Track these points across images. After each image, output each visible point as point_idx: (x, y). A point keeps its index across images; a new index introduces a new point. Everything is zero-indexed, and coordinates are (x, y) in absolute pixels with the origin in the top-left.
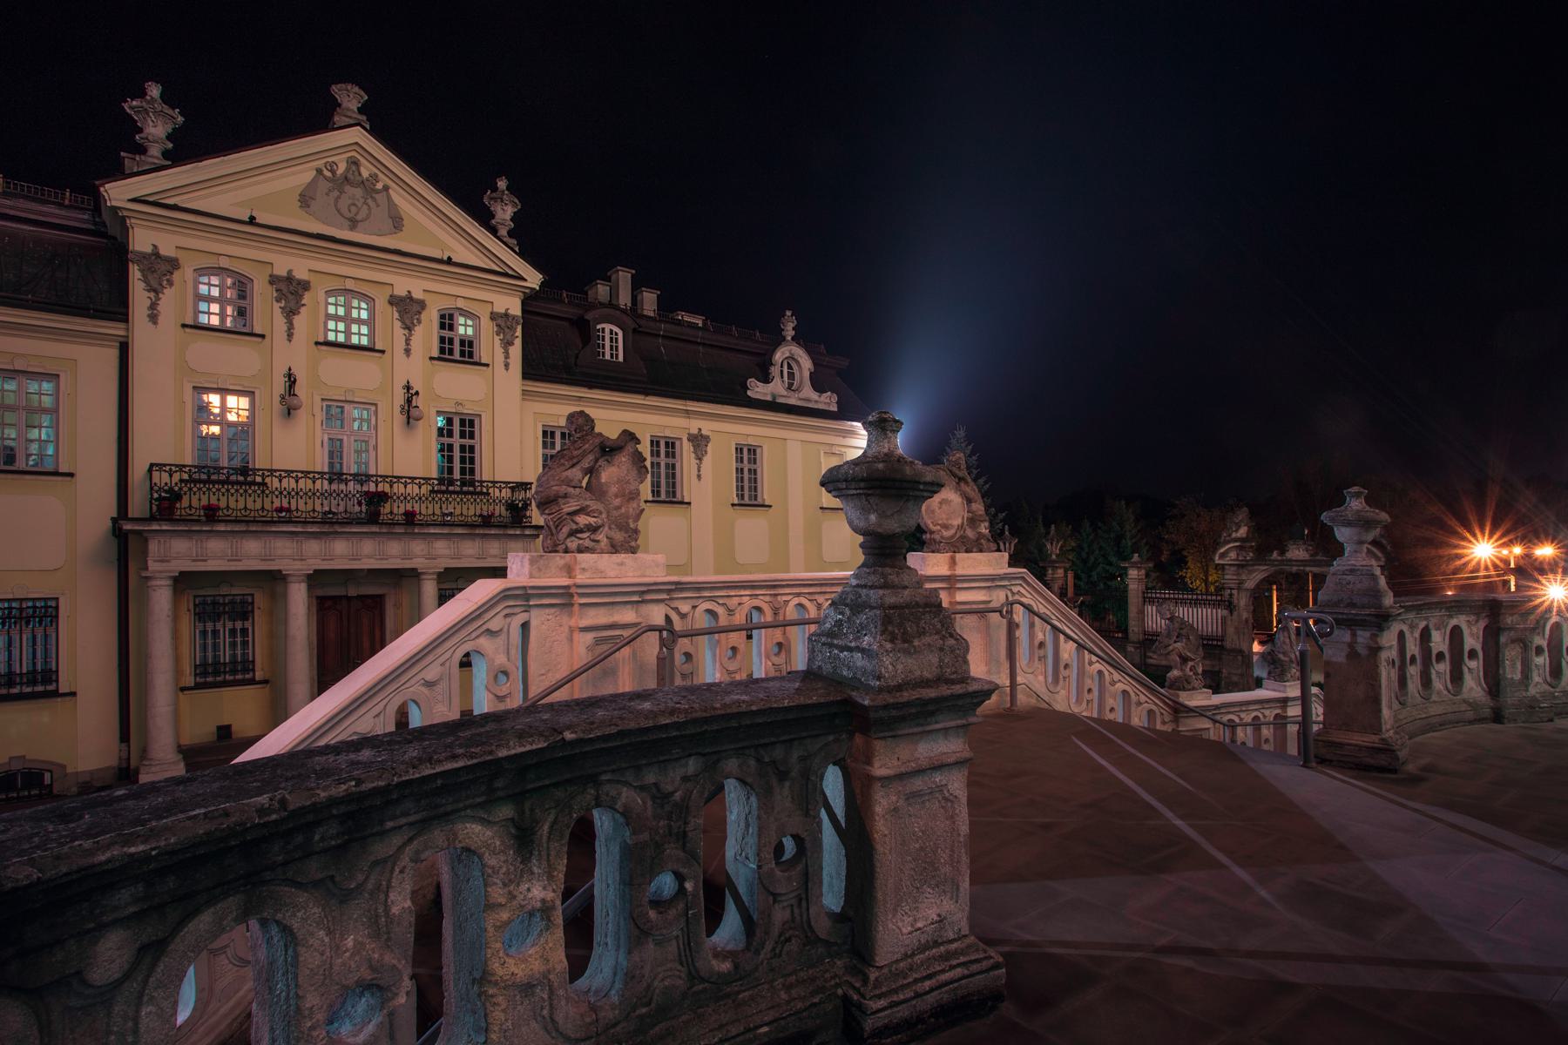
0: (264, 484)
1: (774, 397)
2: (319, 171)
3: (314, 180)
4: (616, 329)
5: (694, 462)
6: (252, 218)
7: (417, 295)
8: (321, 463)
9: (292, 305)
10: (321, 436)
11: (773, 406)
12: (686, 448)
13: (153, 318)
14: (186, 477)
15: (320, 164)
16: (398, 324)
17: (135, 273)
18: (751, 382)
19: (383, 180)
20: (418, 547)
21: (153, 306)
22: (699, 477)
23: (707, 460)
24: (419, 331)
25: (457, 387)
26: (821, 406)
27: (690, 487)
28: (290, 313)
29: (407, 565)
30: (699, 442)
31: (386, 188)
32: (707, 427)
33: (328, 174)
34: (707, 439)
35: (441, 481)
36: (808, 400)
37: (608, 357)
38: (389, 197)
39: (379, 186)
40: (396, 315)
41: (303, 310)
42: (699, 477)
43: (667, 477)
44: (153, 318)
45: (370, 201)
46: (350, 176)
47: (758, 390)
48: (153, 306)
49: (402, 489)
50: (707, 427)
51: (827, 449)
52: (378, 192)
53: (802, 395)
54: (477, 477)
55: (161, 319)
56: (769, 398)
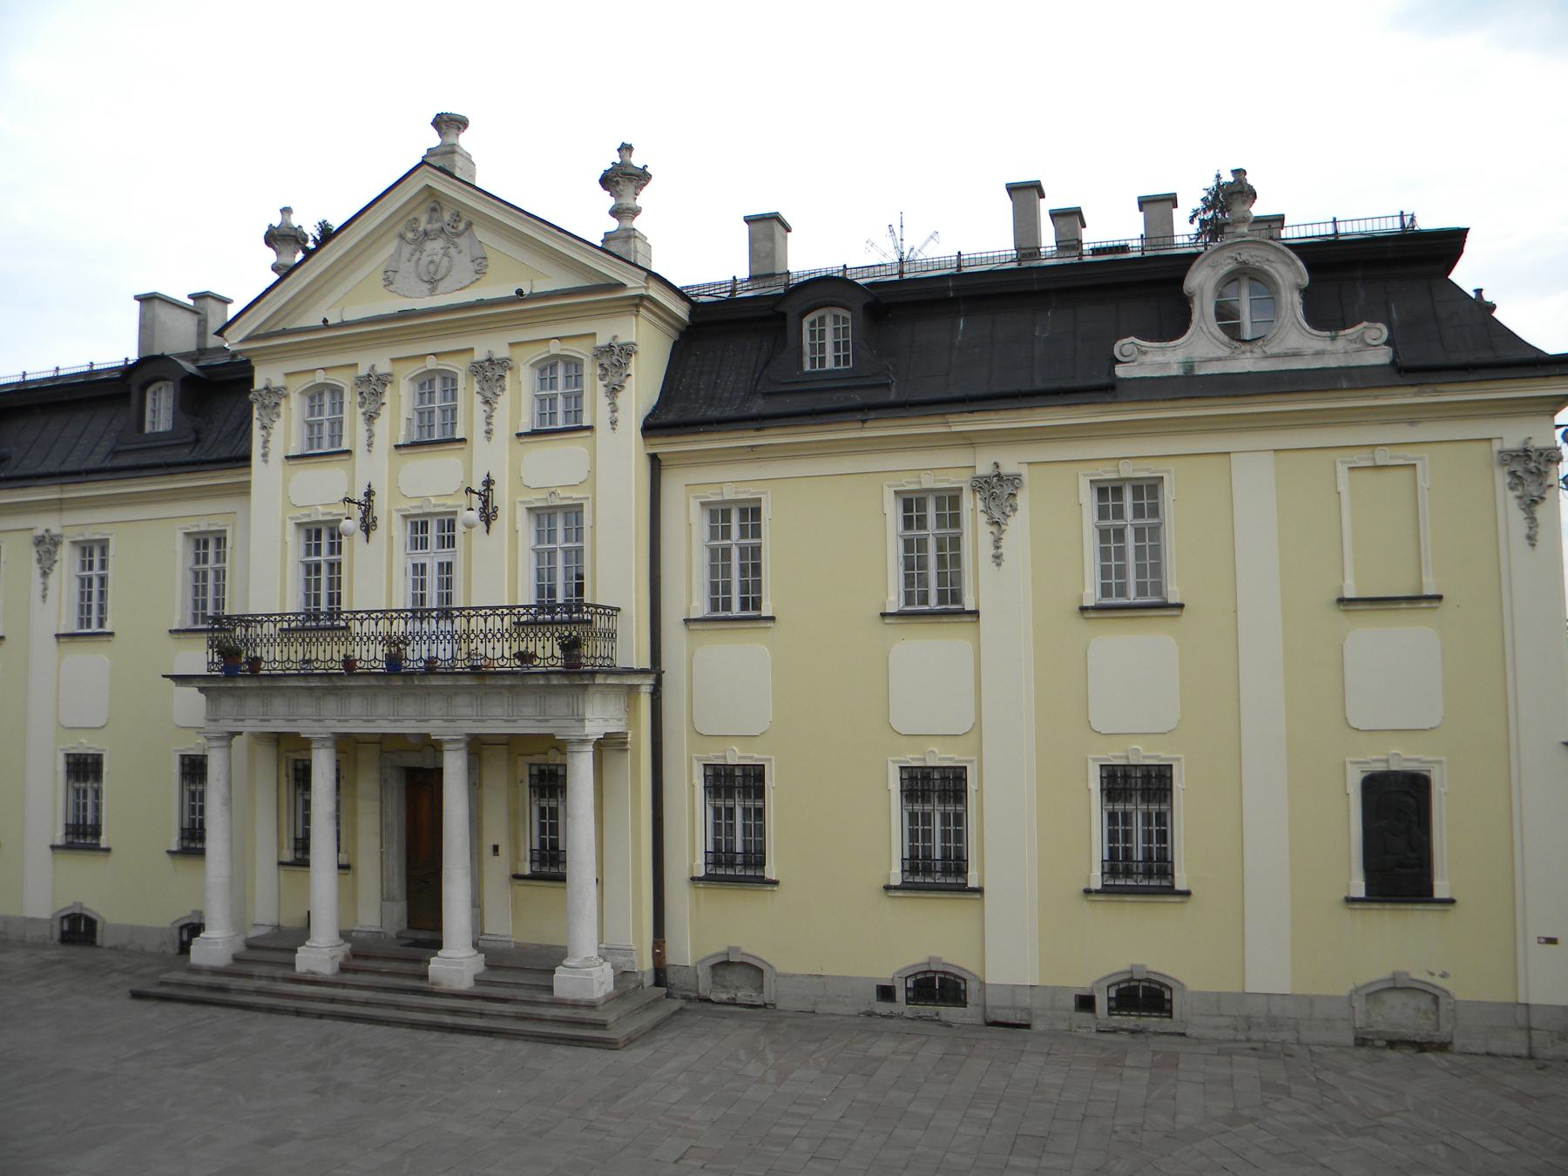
0: (347, 628)
1: (1189, 365)
2: (402, 237)
3: (399, 251)
4: (806, 326)
5: (985, 532)
6: (325, 321)
7: (501, 352)
8: (402, 599)
9: (372, 408)
10: (402, 560)
11: (1190, 386)
12: (970, 505)
13: (265, 455)
14: (286, 625)
15: (401, 227)
16: (478, 399)
17: (256, 414)
18: (1125, 346)
19: (466, 217)
20: (436, 707)
21: (266, 442)
22: (997, 558)
23: (1018, 526)
24: (503, 402)
25: (555, 468)
26: (1331, 362)
27: (982, 584)
28: (370, 418)
29: (423, 728)
30: (998, 490)
31: (469, 225)
32: (1011, 461)
33: (410, 235)
34: (1015, 480)
35: (541, 607)
36: (1296, 354)
37: (807, 368)
38: (473, 235)
39: (462, 226)
40: (477, 388)
41: (385, 411)
42: (997, 558)
43: (923, 565)
44: (265, 455)
45: (453, 251)
46: (429, 227)
47: (1144, 359)
48: (266, 442)
49: (482, 625)
50: (1011, 461)
51: (1362, 459)
52: (458, 235)
53: (1273, 349)
54: (587, 599)
55: (270, 458)
56: (1175, 371)
